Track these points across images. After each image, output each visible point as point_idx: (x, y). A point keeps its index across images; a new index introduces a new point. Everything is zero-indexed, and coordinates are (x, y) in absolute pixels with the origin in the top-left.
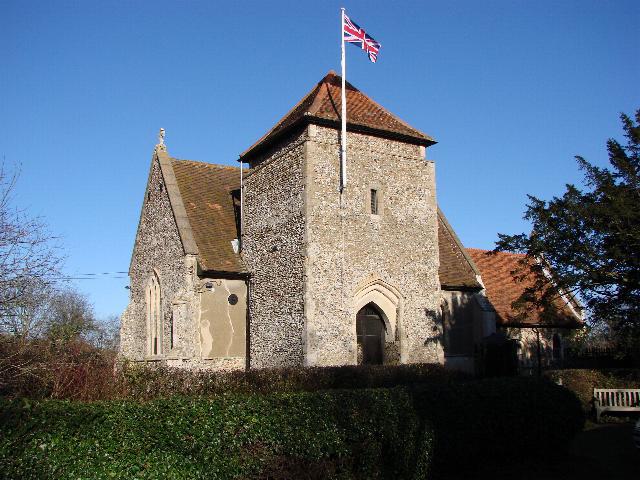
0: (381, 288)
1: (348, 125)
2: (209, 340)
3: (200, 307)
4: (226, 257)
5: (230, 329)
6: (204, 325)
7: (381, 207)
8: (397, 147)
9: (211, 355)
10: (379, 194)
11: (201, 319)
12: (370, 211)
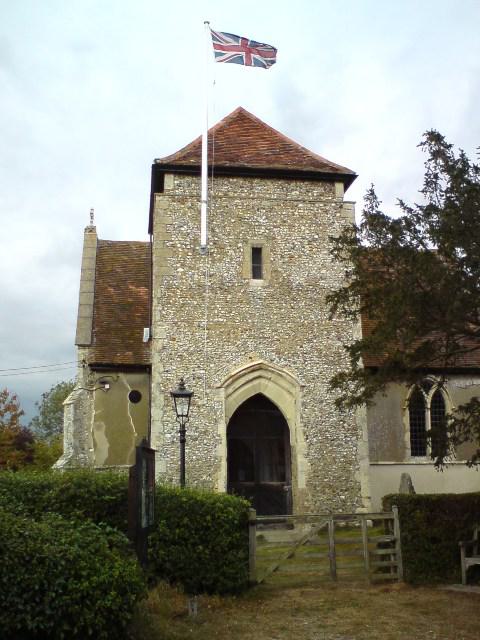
0: (269, 375)
1: (210, 168)
2: (105, 446)
3: (93, 407)
4: (128, 347)
5: (131, 432)
6: (98, 428)
7: (266, 268)
8: (296, 190)
9: (106, 463)
10: (265, 253)
12: (250, 275)
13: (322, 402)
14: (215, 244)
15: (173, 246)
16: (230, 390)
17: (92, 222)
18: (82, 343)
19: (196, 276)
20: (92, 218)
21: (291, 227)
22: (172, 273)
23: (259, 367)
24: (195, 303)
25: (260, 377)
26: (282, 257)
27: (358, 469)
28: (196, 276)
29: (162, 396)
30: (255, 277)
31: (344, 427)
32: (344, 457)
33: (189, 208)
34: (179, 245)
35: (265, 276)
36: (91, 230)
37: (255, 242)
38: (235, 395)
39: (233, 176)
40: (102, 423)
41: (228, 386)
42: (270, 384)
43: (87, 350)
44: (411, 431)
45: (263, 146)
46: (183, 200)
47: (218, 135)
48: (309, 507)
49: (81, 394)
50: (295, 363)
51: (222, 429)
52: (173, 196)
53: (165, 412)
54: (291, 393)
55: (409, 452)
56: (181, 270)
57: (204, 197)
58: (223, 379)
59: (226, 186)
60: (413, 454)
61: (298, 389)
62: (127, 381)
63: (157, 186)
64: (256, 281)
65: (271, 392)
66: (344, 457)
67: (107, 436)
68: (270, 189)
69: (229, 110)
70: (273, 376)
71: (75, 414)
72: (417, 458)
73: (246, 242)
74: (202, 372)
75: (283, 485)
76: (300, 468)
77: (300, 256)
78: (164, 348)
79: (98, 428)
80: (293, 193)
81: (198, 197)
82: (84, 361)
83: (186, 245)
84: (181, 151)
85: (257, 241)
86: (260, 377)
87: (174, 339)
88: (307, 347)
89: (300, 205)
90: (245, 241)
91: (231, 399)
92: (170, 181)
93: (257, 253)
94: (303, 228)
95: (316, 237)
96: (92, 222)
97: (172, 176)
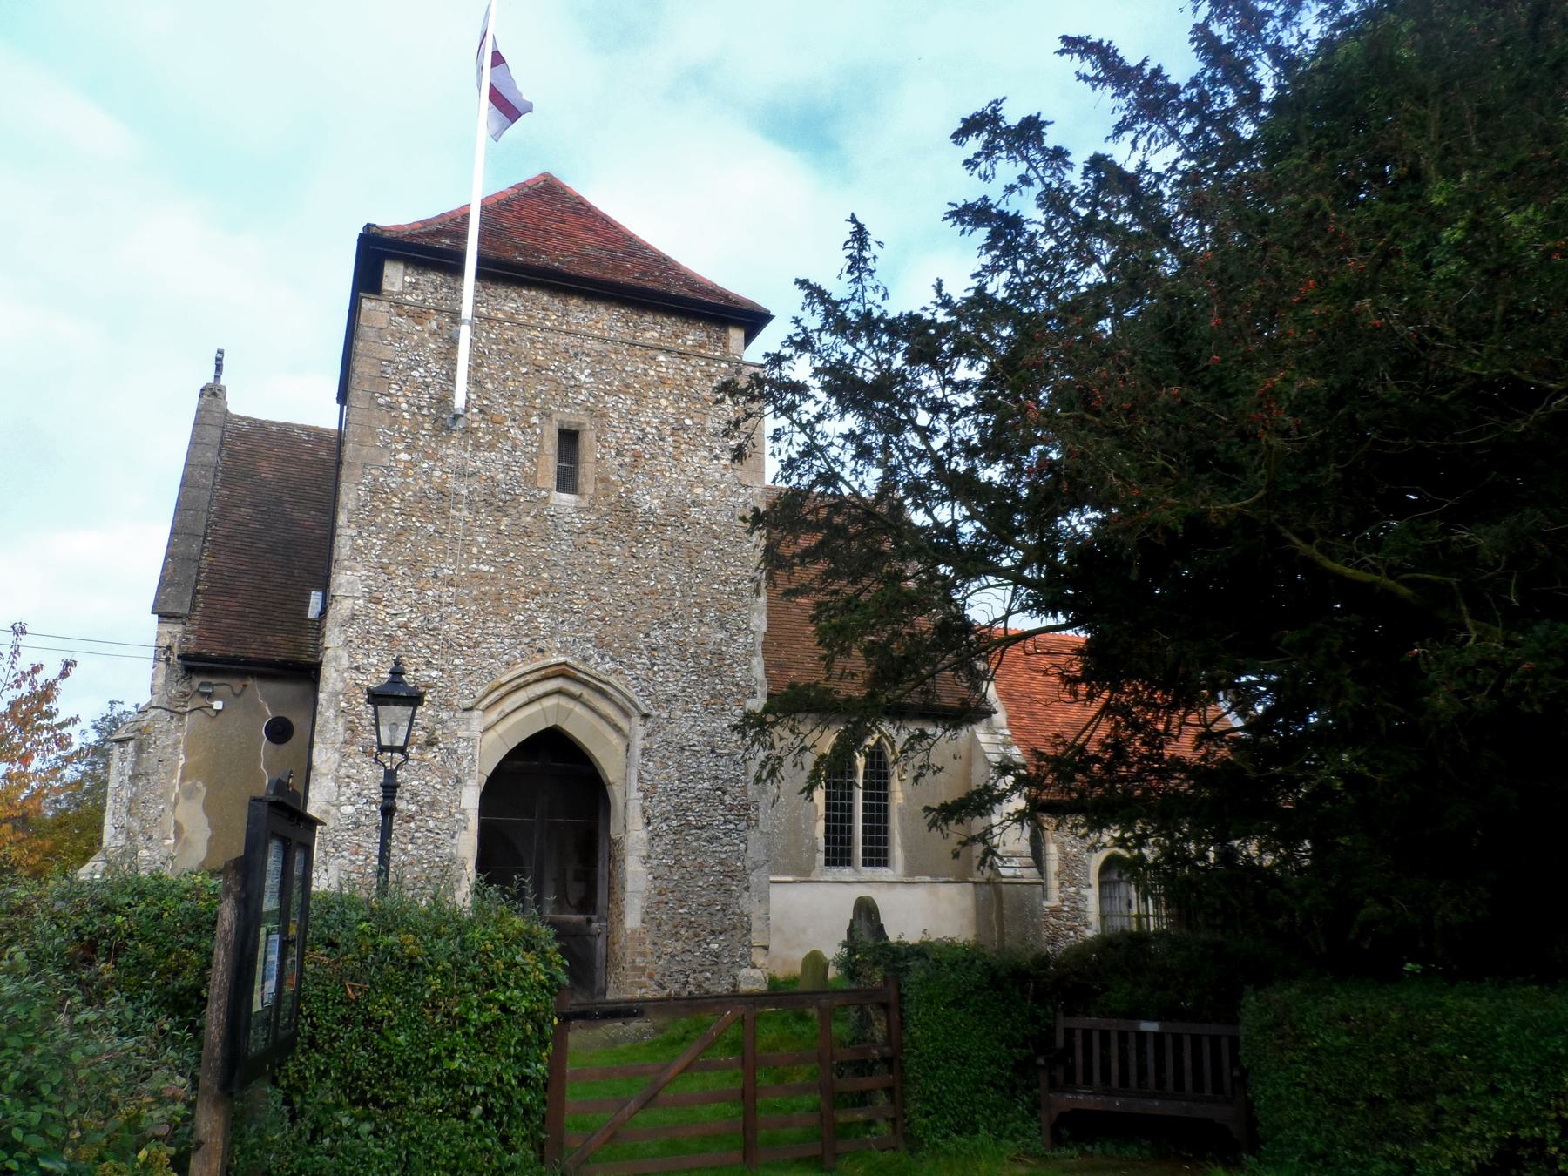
0: (575, 689)
1: (482, 261)
6: (189, 794)
8: (653, 330)
10: (588, 439)
11: (183, 779)
13: (682, 749)
14: (481, 411)
15: (391, 406)
16: (493, 716)
17: (217, 378)
18: (169, 609)
19: (437, 473)
20: (219, 368)
21: (640, 397)
22: (386, 460)
23: (563, 672)
24: (431, 527)
25: (559, 692)
26: (619, 454)
27: (747, 889)
28: (437, 473)
29: (341, 721)
30: (560, 489)
31: (722, 802)
32: (721, 863)
33: (432, 333)
34: (404, 406)
35: (581, 489)
36: (212, 393)
37: (566, 419)
38: (500, 728)
39: (530, 285)
40: (200, 784)
41: (488, 707)
42: (578, 709)
43: (178, 628)
44: (827, 819)
45: (590, 245)
46: (419, 315)
47: (495, 210)
48: (643, 969)
49: (155, 720)
50: (631, 667)
51: (470, 798)
52: (399, 305)
53: (344, 757)
54: (617, 729)
55: (821, 857)
56: (404, 456)
57: (467, 310)
58: (480, 691)
59: (511, 302)
60: (827, 863)
61: (637, 720)
62: (265, 699)
63: (367, 280)
64: (565, 496)
65: (581, 725)
66: (721, 863)
67: (207, 814)
68: (604, 320)
69: (528, 172)
70: (587, 694)
71: (137, 764)
72: (835, 870)
73: (549, 416)
74: (434, 674)
75: (589, 921)
76: (629, 886)
77: (653, 457)
78: (353, 617)
79: (189, 794)
80: (648, 334)
81: (455, 317)
82: (169, 648)
83: (420, 408)
84: (425, 223)
85: (571, 417)
86: (559, 692)
87: (378, 601)
88: (657, 635)
89: (661, 358)
90: (545, 414)
91: (492, 734)
92: (395, 277)
93: (569, 439)
94: (664, 402)
95: (688, 422)
96: (217, 378)
97: (401, 267)
